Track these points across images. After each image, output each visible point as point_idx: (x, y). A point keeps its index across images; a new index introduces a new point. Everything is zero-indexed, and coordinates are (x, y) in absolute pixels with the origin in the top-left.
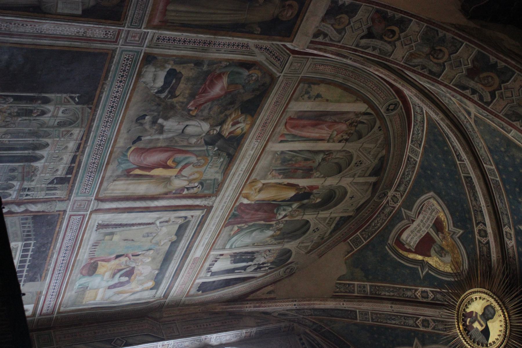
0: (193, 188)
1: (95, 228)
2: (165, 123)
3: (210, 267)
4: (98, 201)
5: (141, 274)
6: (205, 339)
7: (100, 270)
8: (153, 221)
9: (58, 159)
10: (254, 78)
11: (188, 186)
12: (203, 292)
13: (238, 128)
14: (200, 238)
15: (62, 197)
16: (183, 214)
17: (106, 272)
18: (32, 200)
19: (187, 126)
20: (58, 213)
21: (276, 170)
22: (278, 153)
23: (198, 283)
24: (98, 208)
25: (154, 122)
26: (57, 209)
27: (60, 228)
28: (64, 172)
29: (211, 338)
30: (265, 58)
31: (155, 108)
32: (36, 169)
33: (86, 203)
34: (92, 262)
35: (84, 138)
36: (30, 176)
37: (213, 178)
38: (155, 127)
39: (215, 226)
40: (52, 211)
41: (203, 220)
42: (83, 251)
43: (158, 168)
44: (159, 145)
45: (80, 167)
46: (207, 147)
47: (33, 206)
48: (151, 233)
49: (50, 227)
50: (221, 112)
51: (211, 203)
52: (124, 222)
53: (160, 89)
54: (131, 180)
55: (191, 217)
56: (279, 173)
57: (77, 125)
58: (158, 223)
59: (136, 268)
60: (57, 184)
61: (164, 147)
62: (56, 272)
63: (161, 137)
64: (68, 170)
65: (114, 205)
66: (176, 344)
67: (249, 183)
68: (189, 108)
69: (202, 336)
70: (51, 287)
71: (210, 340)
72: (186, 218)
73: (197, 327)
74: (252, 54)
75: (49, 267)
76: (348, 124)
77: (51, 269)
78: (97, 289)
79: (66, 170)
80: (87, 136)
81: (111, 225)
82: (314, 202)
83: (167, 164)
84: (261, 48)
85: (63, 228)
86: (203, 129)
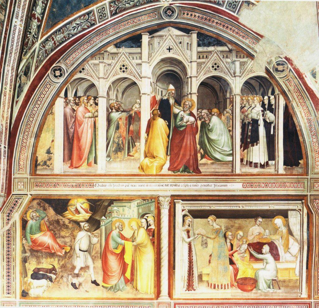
1: (193, 291)
4: (159, 297)
7: (250, 274)
10: (34, 214)
13: (82, 208)
21: (128, 153)
22: (108, 159)
25: (78, 275)
30: (17, 213)
31: (65, 279)
34: (236, 284)
37: (136, 208)
43: (124, 259)
46: (102, 226)
50: (67, 227)
52: (186, 268)
53: (48, 280)
56: (133, 148)
67: (144, 171)
68: (64, 254)
74: (14, 224)
76: (77, 107)
82: (173, 92)
83: (119, 253)
84: (8, 220)
86: (83, 235)
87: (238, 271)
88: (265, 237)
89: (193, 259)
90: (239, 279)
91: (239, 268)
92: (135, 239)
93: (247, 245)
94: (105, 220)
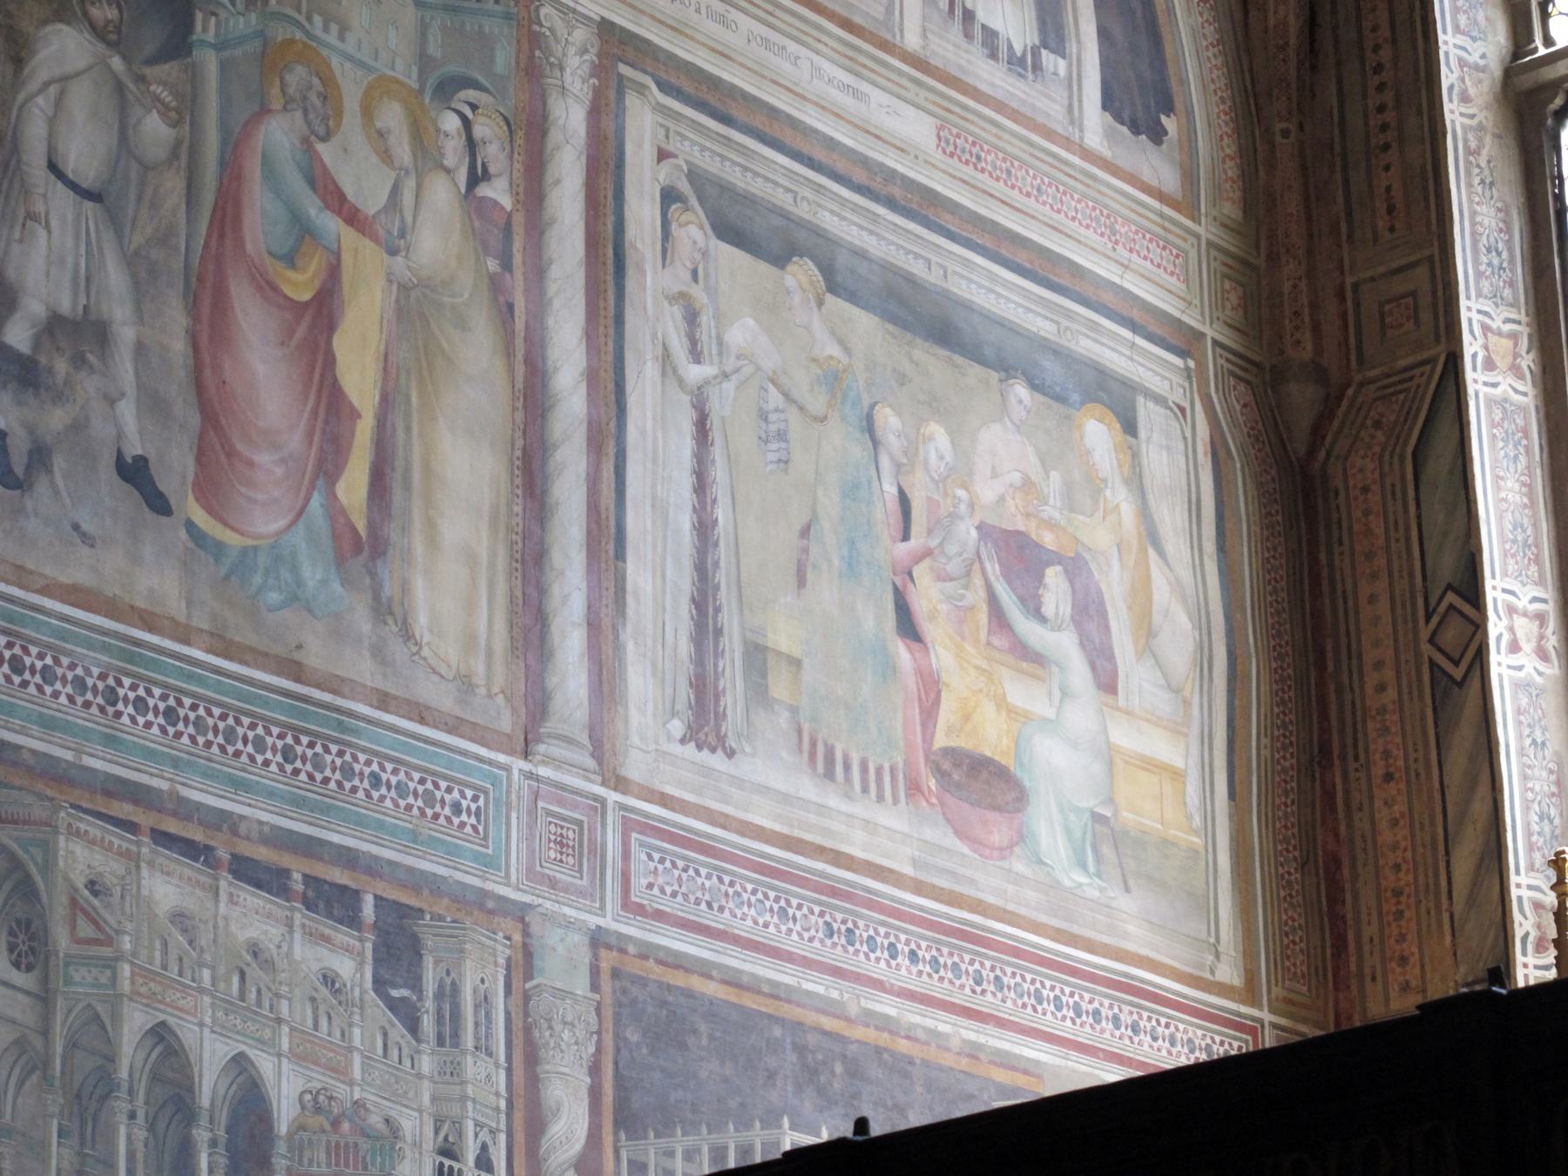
0: (471, 145)
1: (717, 761)
2: (34, 307)
3: (1003, 53)
4: (539, 740)
5: (1027, 485)
6: (1465, 99)
8: (686, 399)
9: (254, 972)
11: (462, 176)
12: (1169, 109)
14: (810, 109)
15: (503, 953)
16: (642, 213)
17: (1001, 702)
18: (520, 1138)
19: (53, 167)
20: (606, 984)
23: (1109, 135)
24: (584, 738)
26: (581, 987)
27: (704, 969)
28: (344, 936)
29: (1462, 63)
32: (315, 1103)
33: (549, 813)
34: (933, 783)
35: (124, 810)
36: (364, 1145)
38: (61, 366)
39: (734, 15)
40: (593, 1019)
41: (688, 87)
42: (859, 835)
43: (330, 361)
44: (179, 346)
45: (310, 838)
47: (556, 1129)
48: (764, 416)
49: (695, 1032)
51: (580, 34)
52: (683, 581)
54: (405, 530)
55: (667, 165)
57: (38, 853)
58: (695, 373)
59: (991, 520)
60: (416, 984)
61: (195, 316)
62: (988, 1002)
63: (126, 334)
64: (330, 915)
65: (570, 642)
66: (1485, 284)
69: (1448, 117)
70: (1084, 1035)
71: (1477, 68)
72: (669, 197)
73: (1386, 147)
75: (955, 1043)
77: (971, 1032)
78: (1111, 764)
79: (326, 927)
80: (108, 794)
81: (699, 659)
83: (307, 304)
85: (706, 954)
86: (81, 64)
87: (939, 692)
92: (402, 235)
94: (223, 14)
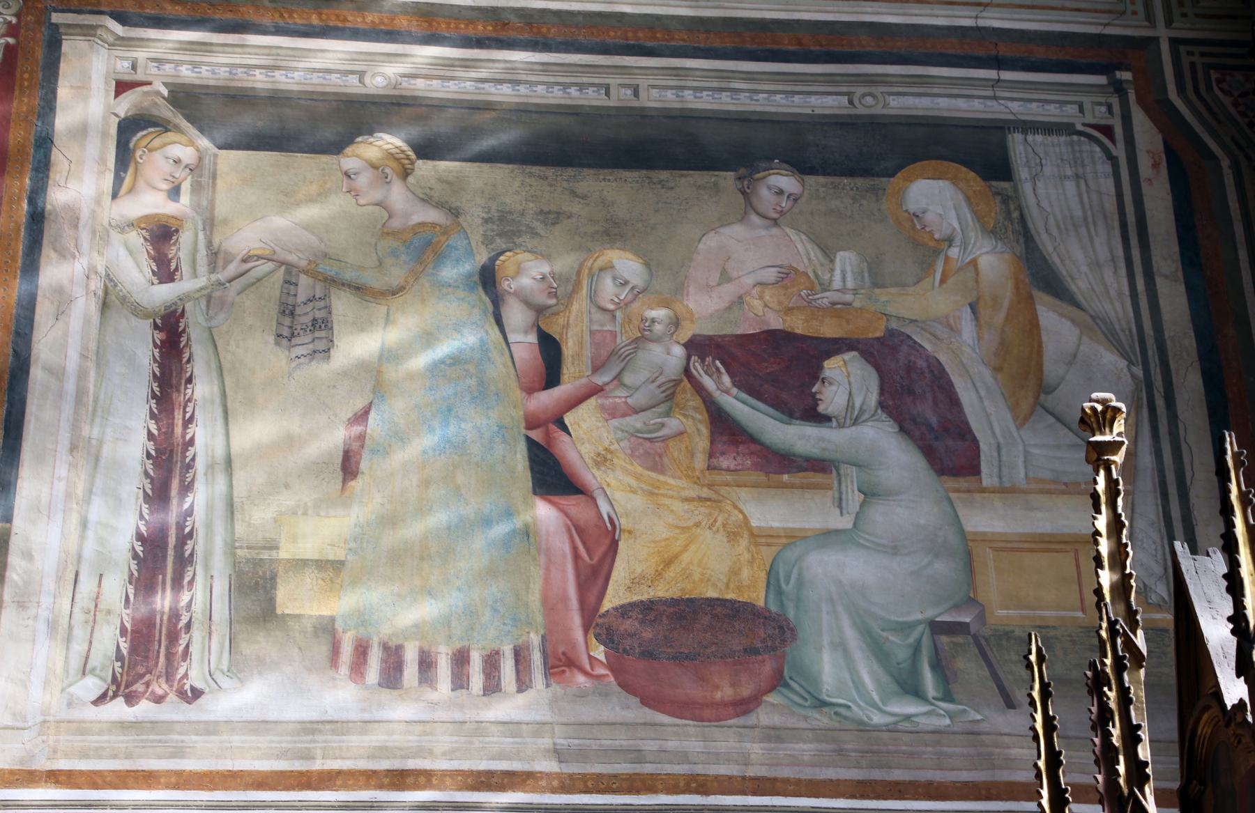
1: (173, 711)
5: (788, 276)
34: (599, 652)
87: (614, 546)
88: (831, 296)
89: (191, 442)
90: (624, 611)
91: (624, 522)
93: (678, 351)
